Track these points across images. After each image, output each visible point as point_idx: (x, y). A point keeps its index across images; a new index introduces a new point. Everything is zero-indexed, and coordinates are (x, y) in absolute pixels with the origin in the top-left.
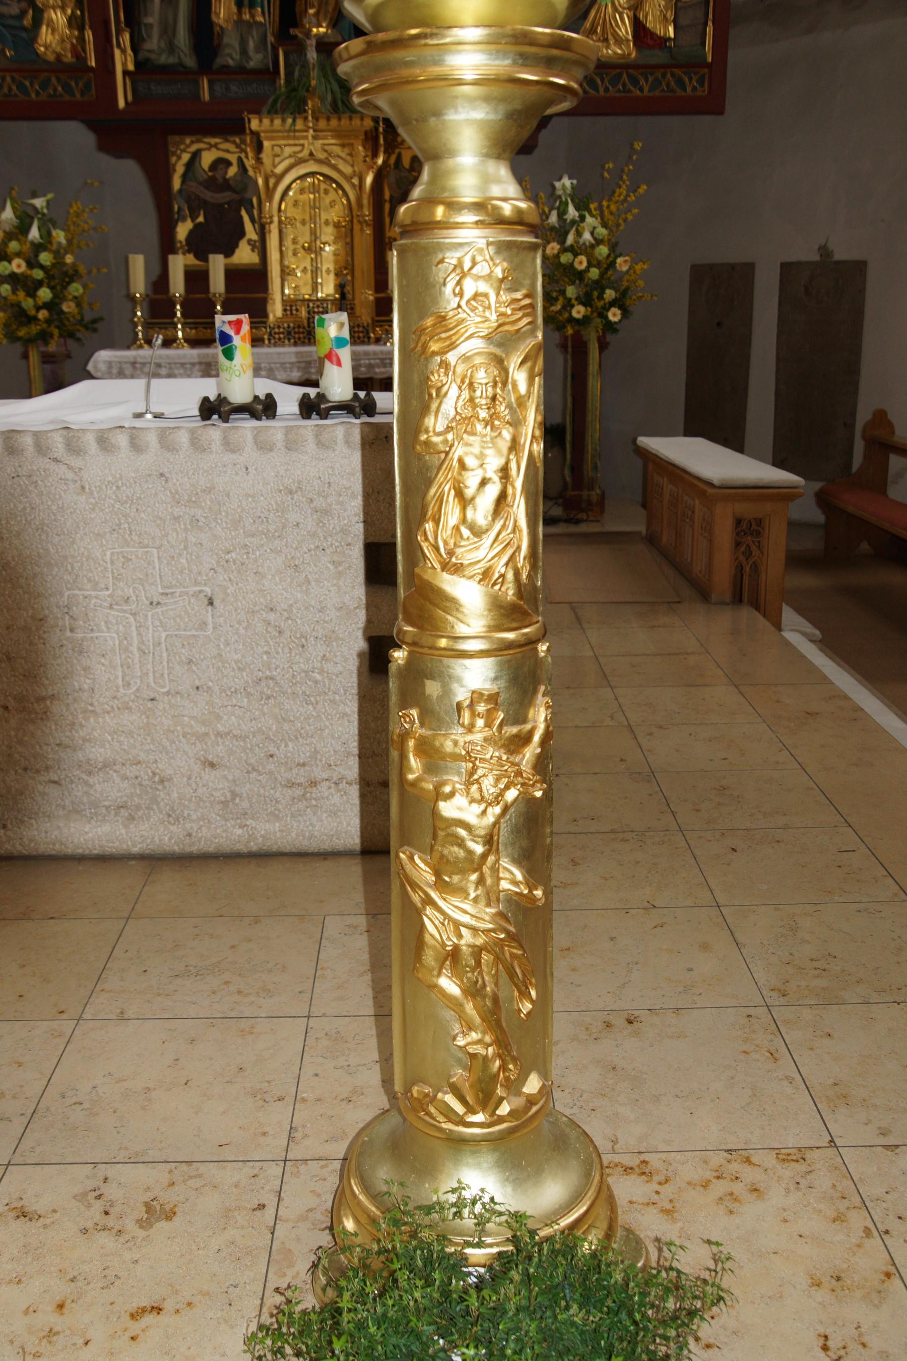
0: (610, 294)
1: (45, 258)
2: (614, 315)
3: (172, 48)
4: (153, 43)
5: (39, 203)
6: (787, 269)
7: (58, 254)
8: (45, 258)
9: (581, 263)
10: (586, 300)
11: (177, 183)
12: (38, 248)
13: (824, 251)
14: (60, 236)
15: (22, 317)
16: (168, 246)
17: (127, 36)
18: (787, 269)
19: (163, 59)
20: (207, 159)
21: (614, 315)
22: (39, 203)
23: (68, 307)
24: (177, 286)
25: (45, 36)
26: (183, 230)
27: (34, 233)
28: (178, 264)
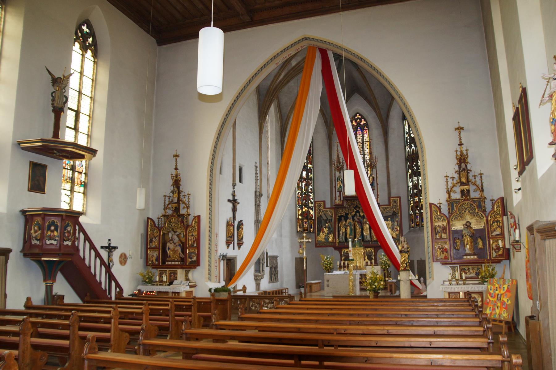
0: (387, 265)
1: (329, 262)
2: (388, 267)
3: (342, 240)
4: (341, 240)
5: (329, 256)
6: (418, 261)
7: (330, 261)
8: (329, 262)
9: (384, 262)
10: (385, 266)
11: (342, 253)
12: (328, 261)
13: (421, 259)
14: (330, 260)
15: (326, 267)
16: (341, 260)
17: (338, 239)
18: (418, 261)
19: (342, 241)
20: (346, 251)
21: (388, 267)
22: (329, 256)
23: (331, 267)
24: (342, 264)
25: (330, 240)
26: (343, 258)
27: (328, 259)
28: (342, 263)
